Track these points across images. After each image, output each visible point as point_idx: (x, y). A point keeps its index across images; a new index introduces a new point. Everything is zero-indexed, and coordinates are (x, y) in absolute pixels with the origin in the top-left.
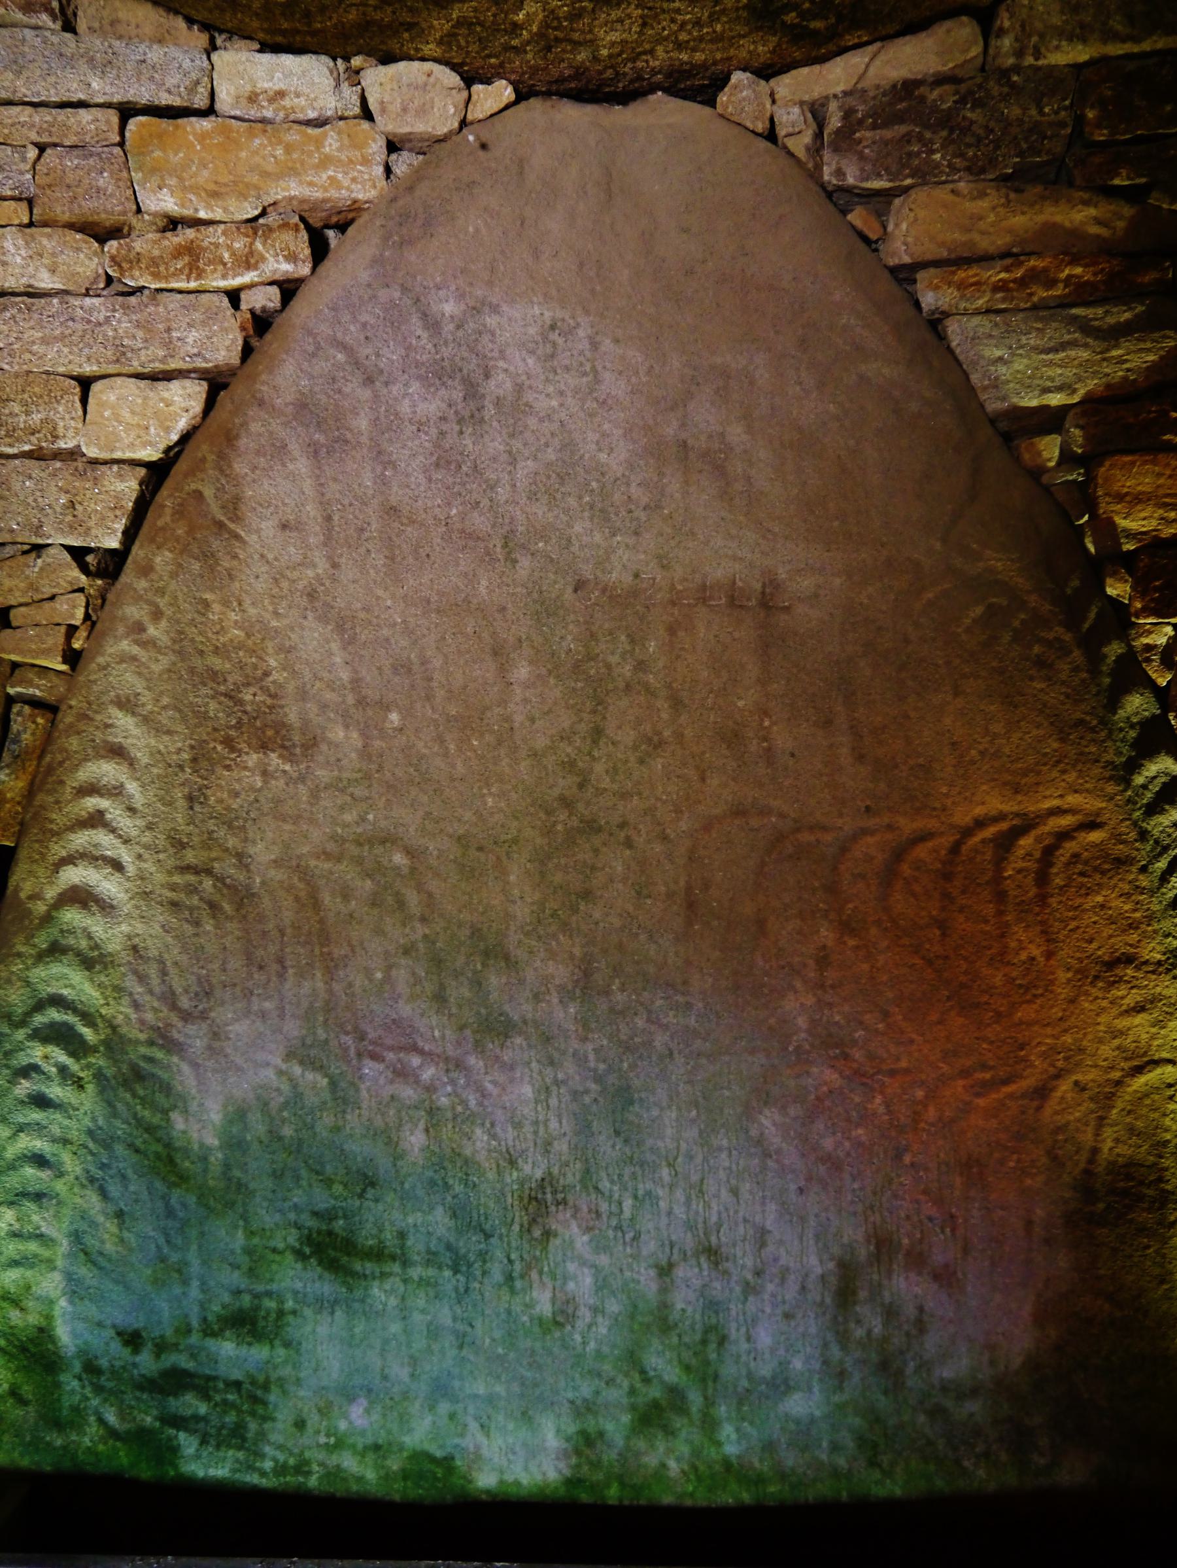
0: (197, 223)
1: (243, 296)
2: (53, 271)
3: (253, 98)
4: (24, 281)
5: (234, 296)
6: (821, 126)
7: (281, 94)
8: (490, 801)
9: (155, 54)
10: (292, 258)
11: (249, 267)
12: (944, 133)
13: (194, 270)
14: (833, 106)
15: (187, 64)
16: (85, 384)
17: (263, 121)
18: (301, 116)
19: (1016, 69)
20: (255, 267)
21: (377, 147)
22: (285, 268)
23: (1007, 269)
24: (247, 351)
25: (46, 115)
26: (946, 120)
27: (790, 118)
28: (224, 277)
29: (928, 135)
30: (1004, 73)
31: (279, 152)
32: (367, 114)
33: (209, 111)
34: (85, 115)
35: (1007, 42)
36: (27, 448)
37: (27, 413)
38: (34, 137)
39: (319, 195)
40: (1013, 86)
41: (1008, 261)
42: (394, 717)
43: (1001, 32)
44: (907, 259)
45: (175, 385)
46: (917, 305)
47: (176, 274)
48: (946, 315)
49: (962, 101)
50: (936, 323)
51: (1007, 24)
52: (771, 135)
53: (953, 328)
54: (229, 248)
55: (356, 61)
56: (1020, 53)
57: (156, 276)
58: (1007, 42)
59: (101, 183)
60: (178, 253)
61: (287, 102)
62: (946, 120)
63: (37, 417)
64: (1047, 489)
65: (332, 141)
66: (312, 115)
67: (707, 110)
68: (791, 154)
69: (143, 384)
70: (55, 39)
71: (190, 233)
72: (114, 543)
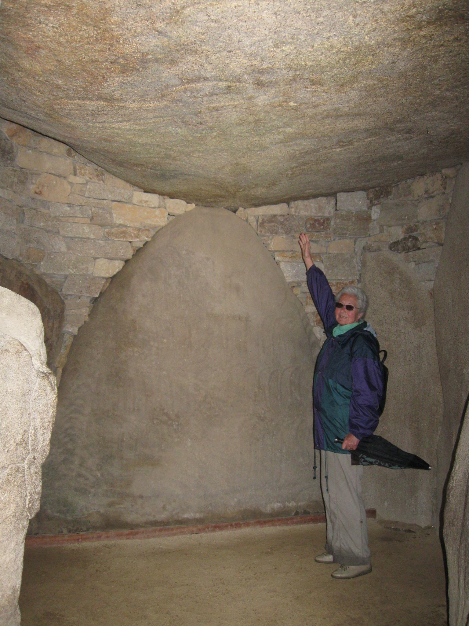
0: (126, 226)
1: (133, 243)
2: (94, 234)
3: (141, 201)
4: (87, 236)
5: (130, 242)
6: (257, 221)
7: (147, 201)
8: (185, 360)
9: (122, 191)
10: (147, 237)
11: (137, 238)
12: (281, 226)
13: (124, 237)
14: (260, 217)
15: (129, 193)
16: (95, 259)
17: (142, 206)
18: (151, 206)
19: (295, 215)
20: (139, 238)
21: (166, 214)
22: (146, 239)
23: (292, 254)
24: (133, 255)
25: (98, 201)
26: (281, 223)
27: (251, 219)
28: (132, 239)
29: (278, 226)
30: (293, 215)
31: (146, 213)
32: (165, 208)
33: (131, 203)
34: (105, 201)
35: (293, 210)
36: (81, 273)
37: (83, 265)
38: (94, 205)
39: (154, 223)
40: (294, 219)
41: (292, 252)
42: (165, 340)
43: (292, 207)
44: (273, 250)
45: (116, 262)
46: (274, 259)
47: (121, 238)
48: (280, 261)
49: (285, 220)
50: (278, 263)
51: (293, 206)
52: (247, 220)
53: (282, 265)
54: (133, 233)
55: (166, 197)
56: (295, 212)
57: (116, 237)
58: (293, 210)
59: (107, 216)
60: (121, 233)
61: (148, 203)
62: (281, 223)
63: (84, 266)
64: (298, 298)
65: (157, 212)
66: (153, 206)
67: (234, 213)
68: (250, 224)
69: (109, 260)
70: (103, 186)
71: (124, 229)
72: (97, 296)
